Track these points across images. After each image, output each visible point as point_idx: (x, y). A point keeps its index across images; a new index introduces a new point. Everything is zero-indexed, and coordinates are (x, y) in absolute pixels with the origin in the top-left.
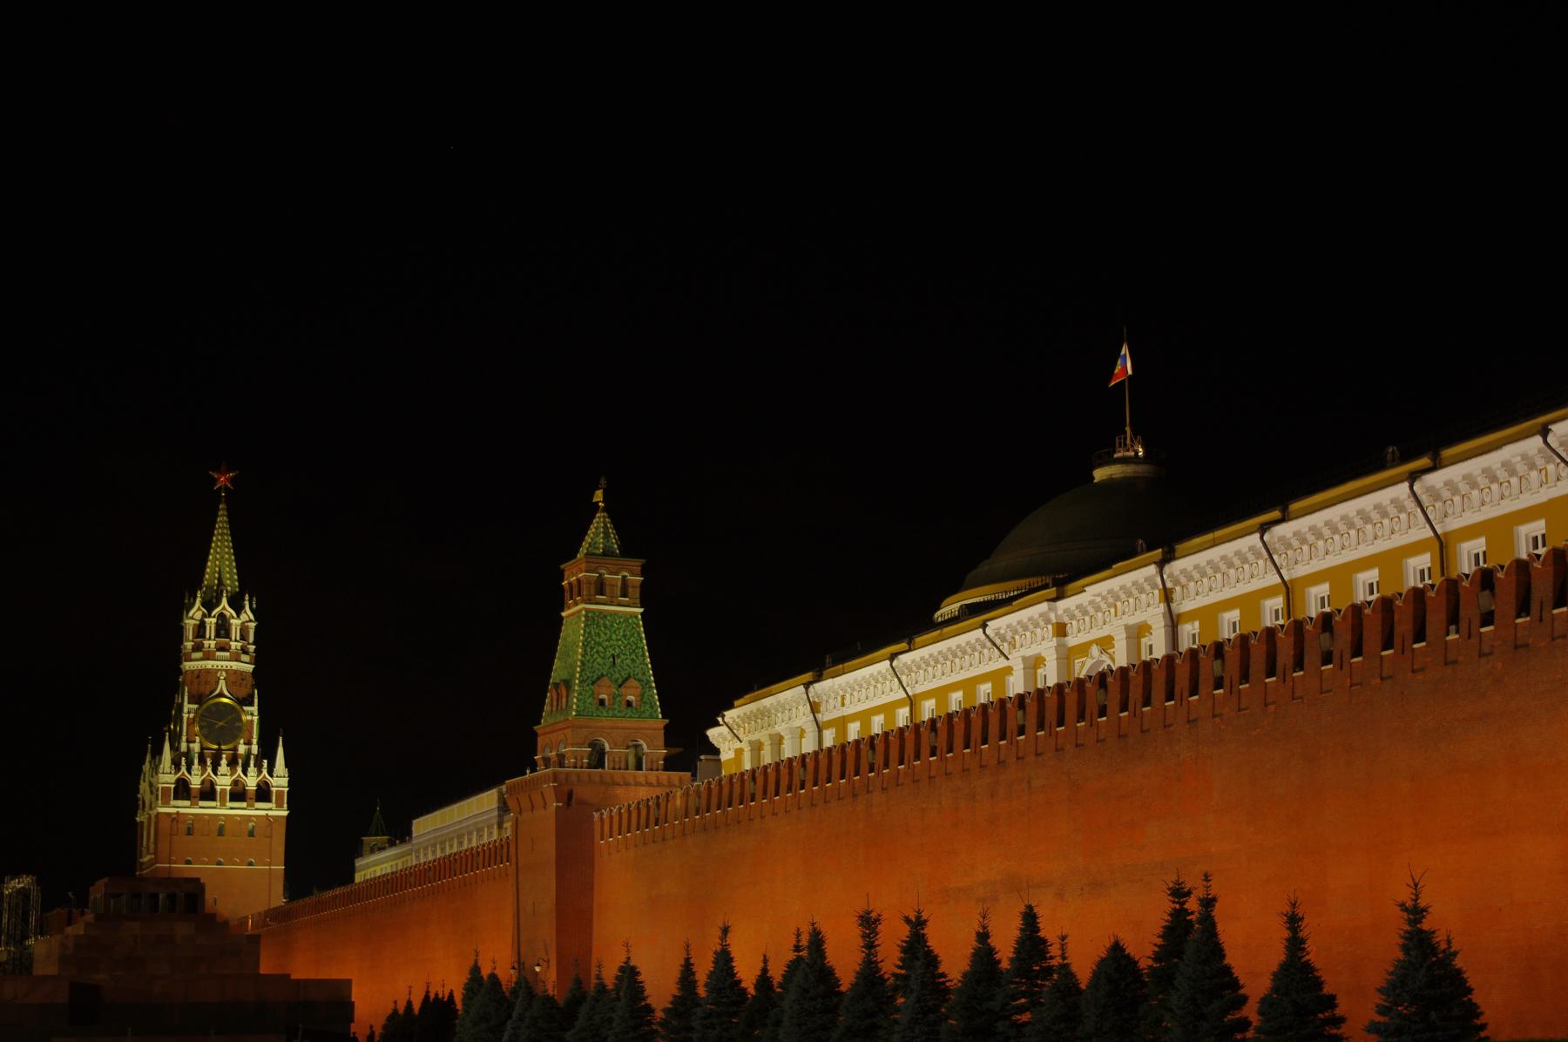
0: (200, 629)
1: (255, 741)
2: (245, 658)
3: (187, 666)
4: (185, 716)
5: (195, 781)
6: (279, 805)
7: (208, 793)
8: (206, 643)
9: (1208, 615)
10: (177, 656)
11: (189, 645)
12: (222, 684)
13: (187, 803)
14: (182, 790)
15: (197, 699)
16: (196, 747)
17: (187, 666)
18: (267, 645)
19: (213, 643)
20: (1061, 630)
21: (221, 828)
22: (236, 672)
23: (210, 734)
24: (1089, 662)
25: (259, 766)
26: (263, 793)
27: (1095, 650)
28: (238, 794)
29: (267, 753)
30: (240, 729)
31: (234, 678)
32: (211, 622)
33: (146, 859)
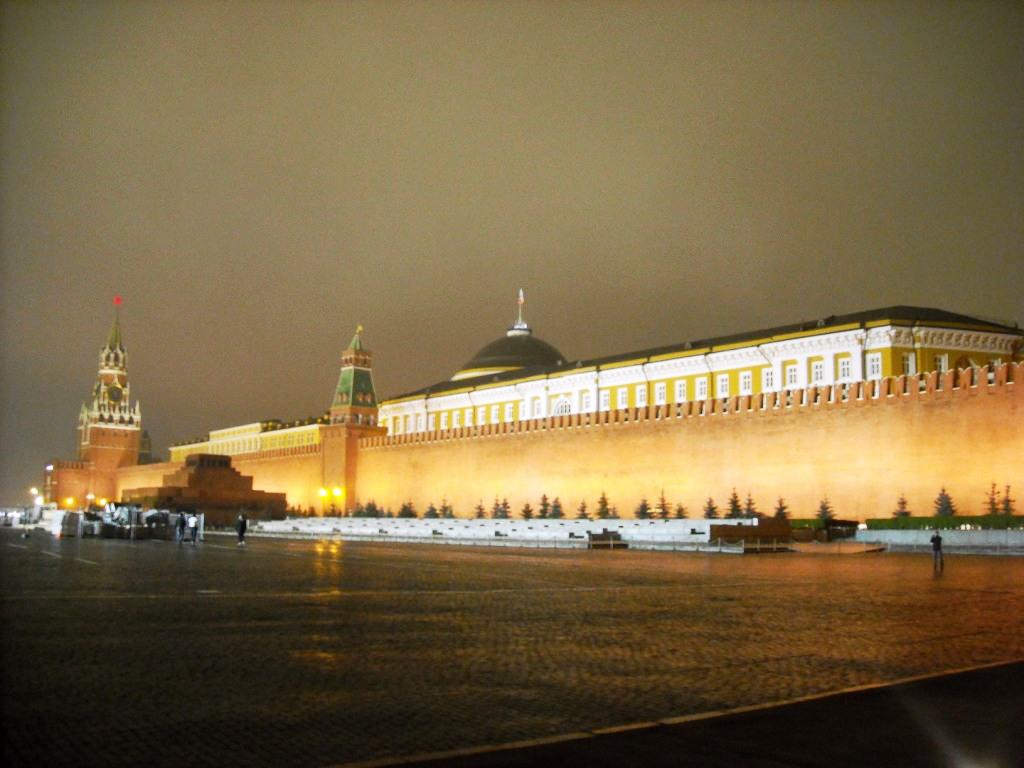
3: (102, 372)
5: (106, 415)
7: (111, 420)
9: (613, 390)
10: (98, 368)
12: (116, 380)
14: (101, 419)
15: (106, 384)
16: (106, 402)
20: (547, 389)
21: (115, 434)
24: (558, 400)
26: (131, 421)
27: (562, 397)
28: (122, 421)
29: (132, 405)
32: (112, 356)
33: (83, 444)
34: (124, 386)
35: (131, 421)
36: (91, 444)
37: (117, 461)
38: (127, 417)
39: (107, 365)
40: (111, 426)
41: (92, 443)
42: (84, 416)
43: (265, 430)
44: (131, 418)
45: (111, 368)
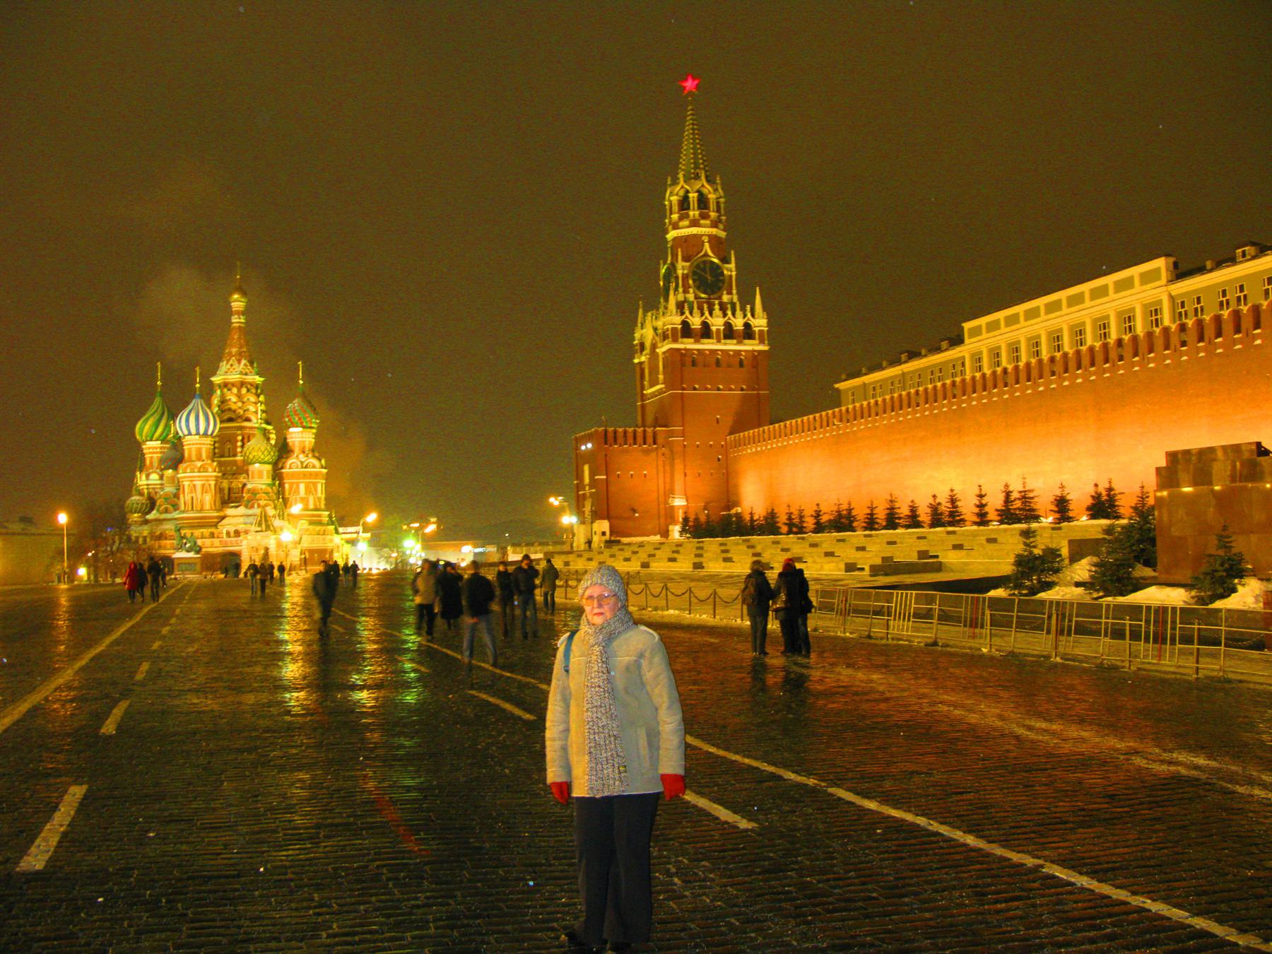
0: (684, 204)
1: (734, 291)
2: (721, 226)
4: (680, 272)
5: (696, 322)
6: (762, 342)
7: (706, 332)
8: (691, 213)
11: (675, 217)
12: (707, 246)
13: (691, 340)
14: (686, 330)
15: (685, 259)
16: (691, 297)
17: (672, 235)
18: (733, 216)
19: (697, 213)
21: (717, 361)
22: (716, 236)
23: (702, 285)
25: (743, 310)
26: (748, 333)
28: (729, 333)
29: (746, 300)
30: (723, 281)
31: (714, 240)
32: (693, 196)
34: (725, 260)
35: (748, 333)
36: (668, 387)
37: (728, 422)
38: (738, 323)
39: (681, 219)
40: (708, 345)
41: (670, 384)
42: (645, 333)
43: (1180, 273)
44: (747, 325)
45: (695, 223)
